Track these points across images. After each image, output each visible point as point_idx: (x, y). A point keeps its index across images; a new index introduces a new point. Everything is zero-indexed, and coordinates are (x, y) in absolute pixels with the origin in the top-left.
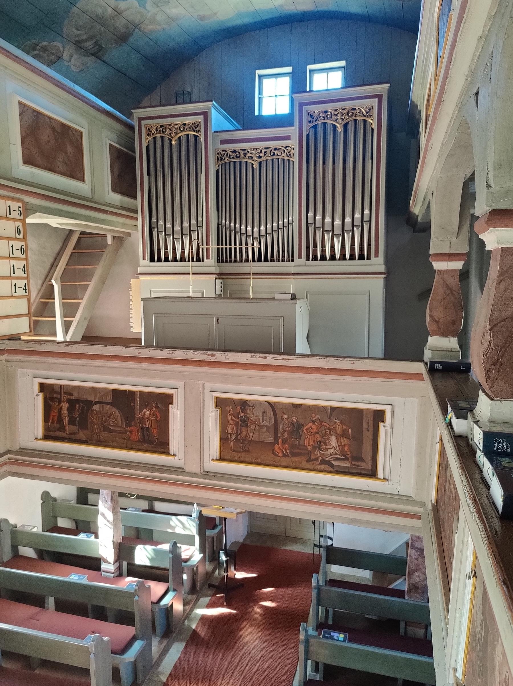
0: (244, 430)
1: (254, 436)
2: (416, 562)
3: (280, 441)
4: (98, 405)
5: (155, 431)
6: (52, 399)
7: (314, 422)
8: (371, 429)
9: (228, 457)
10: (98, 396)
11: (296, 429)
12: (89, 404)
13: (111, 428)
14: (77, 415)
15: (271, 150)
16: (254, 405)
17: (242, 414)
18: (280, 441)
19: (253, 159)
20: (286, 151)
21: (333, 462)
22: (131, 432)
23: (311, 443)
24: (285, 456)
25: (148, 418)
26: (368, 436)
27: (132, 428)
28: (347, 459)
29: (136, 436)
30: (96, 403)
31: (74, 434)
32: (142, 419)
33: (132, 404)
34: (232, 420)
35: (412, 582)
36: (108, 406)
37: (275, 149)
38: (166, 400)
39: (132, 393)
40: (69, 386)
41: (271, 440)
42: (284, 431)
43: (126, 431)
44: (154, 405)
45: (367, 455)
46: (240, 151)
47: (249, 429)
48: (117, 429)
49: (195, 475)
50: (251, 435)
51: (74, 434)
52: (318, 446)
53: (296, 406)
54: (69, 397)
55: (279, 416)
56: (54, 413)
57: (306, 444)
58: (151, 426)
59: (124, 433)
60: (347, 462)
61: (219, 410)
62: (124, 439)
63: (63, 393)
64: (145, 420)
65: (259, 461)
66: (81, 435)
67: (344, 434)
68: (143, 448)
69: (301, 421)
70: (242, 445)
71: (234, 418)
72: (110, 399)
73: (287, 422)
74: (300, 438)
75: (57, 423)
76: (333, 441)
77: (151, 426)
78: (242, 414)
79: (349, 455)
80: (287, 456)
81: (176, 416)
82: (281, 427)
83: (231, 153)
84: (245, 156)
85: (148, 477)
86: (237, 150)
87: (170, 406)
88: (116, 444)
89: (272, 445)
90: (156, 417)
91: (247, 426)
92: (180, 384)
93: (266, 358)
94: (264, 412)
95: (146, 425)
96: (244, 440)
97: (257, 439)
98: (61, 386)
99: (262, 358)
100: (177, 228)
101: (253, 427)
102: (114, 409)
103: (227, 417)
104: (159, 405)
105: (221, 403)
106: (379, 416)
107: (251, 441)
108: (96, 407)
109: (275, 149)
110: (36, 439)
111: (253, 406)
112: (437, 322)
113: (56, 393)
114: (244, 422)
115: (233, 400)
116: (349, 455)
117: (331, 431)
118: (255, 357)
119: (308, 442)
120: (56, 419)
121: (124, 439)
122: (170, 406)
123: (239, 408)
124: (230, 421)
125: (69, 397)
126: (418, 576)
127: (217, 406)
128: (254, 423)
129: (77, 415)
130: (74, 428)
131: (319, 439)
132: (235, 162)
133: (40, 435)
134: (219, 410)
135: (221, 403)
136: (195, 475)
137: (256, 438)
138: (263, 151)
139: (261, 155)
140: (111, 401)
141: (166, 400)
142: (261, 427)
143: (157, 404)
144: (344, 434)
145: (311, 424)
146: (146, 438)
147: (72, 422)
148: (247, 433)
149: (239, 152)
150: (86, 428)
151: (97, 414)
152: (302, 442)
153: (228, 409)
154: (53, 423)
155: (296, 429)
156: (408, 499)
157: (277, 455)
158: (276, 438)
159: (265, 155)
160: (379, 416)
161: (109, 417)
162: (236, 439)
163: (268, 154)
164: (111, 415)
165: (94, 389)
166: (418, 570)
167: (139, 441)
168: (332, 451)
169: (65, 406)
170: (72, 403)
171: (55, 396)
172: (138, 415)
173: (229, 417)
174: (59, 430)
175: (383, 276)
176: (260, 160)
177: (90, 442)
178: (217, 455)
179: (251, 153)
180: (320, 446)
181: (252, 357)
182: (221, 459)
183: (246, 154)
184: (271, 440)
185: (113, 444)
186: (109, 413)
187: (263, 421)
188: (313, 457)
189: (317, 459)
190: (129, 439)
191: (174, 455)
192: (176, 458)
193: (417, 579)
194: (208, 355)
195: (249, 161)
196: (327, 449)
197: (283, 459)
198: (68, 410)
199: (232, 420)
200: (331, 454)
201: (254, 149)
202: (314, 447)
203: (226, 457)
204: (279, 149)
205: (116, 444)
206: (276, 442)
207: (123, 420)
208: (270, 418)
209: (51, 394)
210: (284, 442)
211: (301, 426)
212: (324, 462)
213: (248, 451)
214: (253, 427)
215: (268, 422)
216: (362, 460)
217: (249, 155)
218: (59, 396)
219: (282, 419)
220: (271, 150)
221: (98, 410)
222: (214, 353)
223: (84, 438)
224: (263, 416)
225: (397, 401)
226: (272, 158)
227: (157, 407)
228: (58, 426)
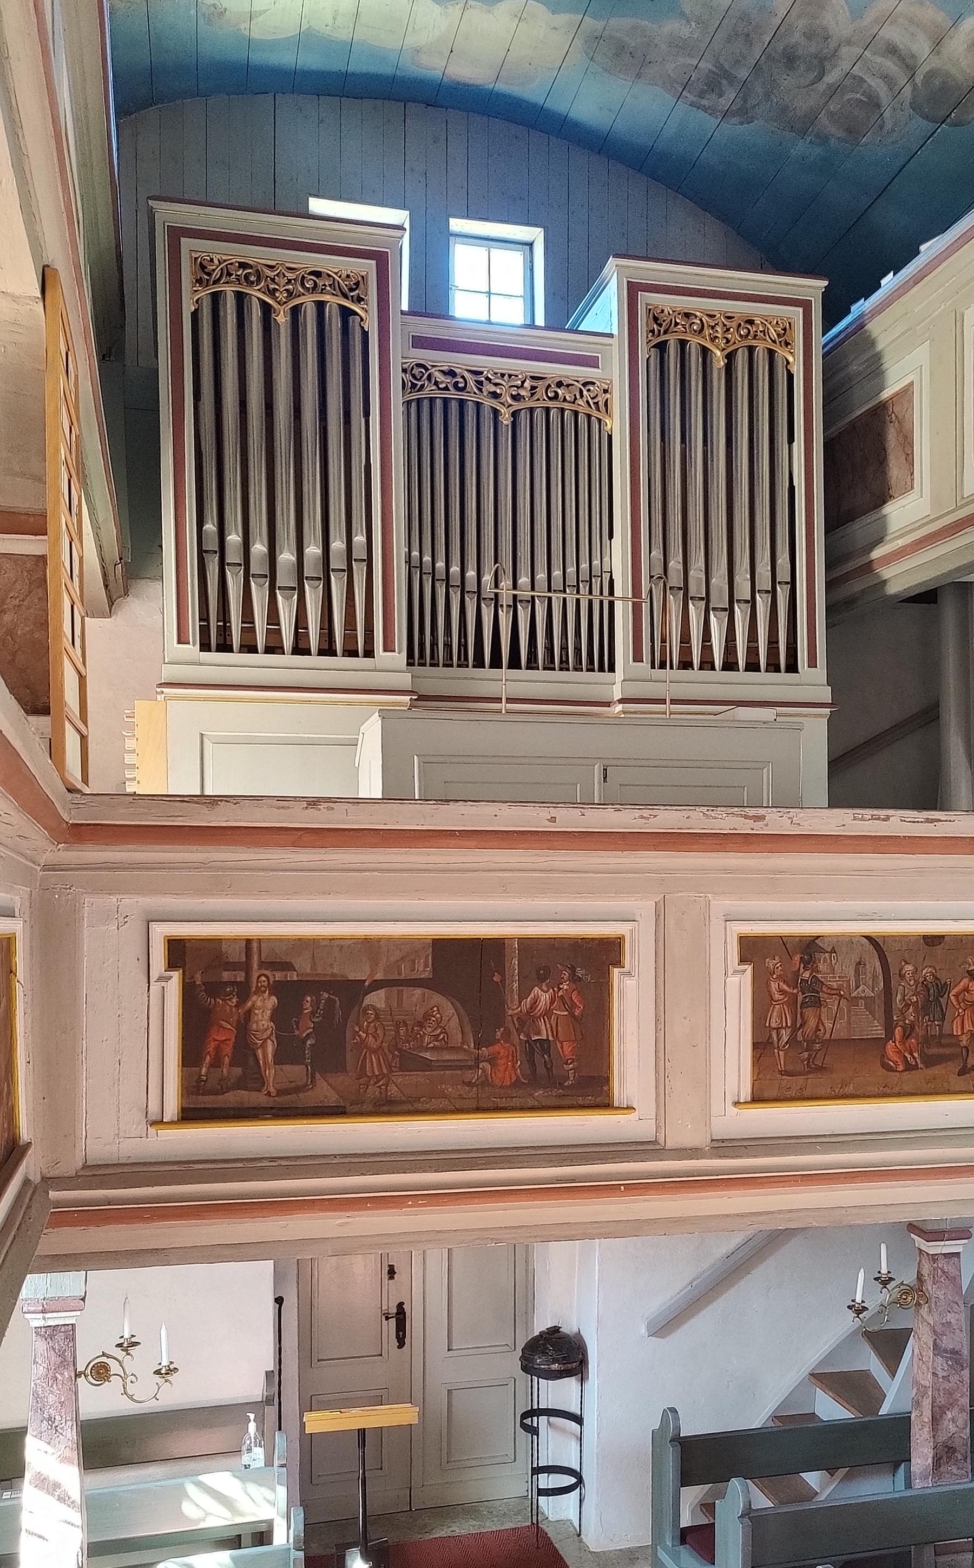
0: (810, 1013)
1: (837, 1026)
4: (382, 993)
5: (567, 1048)
6: (215, 989)
9: (774, 1093)
10: (382, 964)
11: (934, 995)
12: (353, 992)
13: (428, 1055)
14: (306, 1028)
15: (549, 386)
17: (807, 975)
19: (502, 400)
20: (585, 392)
22: (492, 1061)
25: (548, 1013)
27: (497, 1047)
29: (508, 1070)
30: (377, 985)
31: (298, 1090)
32: (528, 1020)
33: (497, 978)
34: (782, 991)
36: (418, 991)
37: (560, 384)
38: (604, 954)
39: (496, 945)
40: (279, 940)
41: (878, 1031)
42: (907, 1006)
43: (478, 1060)
44: (566, 975)
46: (466, 374)
47: (824, 1010)
48: (447, 1056)
49: (693, 1153)
50: (829, 1025)
51: (298, 1090)
53: (932, 941)
54: (279, 976)
55: (894, 970)
56: (223, 1034)
58: (556, 1036)
59: (470, 1068)
61: (749, 969)
62: (469, 1084)
63: (255, 966)
64: (535, 1019)
66: (324, 1091)
68: (531, 1102)
69: (944, 977)
70: (806, 1055)
71: (785, 987)
72: (424, 970)
73: (912, 983)
74: (943, 1019)
75: (231, 1065)
77: (556, 1036)
78: (807, 975)
81: (631, 997)
82: (899, 997)
83: (440, 377)
84: (480, 390)
85: (559, 1180)
86: (457, 371)
87: (616, 971)
88: (444, 1103)
90: (571, 1008)
92: (644, 907)
93: (887, 819)
94: (859, 963)
95: (539, 1033)
96: (811, 1042)
97: (844, 1035)
98: (249, 941)
99: (879, 819)
100: (286, 557)
101: (833, 1003)
102: (437, 999)
103: (768, 986)
104: (580, 972)
105: (751, 949)
107: (830, 1040)
108: (377, 999)
109: (560, 384)
110: (159, 1123)
113: (232, 966)
114: (809, 994)
115: (782, 941)
118: (863, 819)
120: (228, 1050)
121: (469, 1084)
122: (616, 971)
123: (797, 958)
124: (777, 996)
125: (279, 976)
127: (742, 960)
128: (837, 993)
129: (306, 1028)
130: (295, 1072)
132: (446, 401)
133: (172, 1109)
134: (749, 969)
135: (751, 949)
136: (693, 1153)
137: (841, 1030)
138: (527, 384)
139: (523, 393)
140: (427, 974)
141: (604, 954)
142: (853, 1001)
143: (573, 969)
146: (541, 1070)
147: (287, 1053)
149: (463, 377)
150: (341, 1067)
151: (377, 1017)
152: (946, 1030)
153: (770, 963)
154: (216, 1063)
159: (532, 395)
161: (421, 1025)
162: (792, 1040)
163: (540, 392)
164: (427, 1016)
165: (370, 945)
167: (516, 1084)
169: (264, 1006)
170: (290, 994)
171: (226, 976)
172: (515, 1007)
173: (774, 986)
174: (240, 1084)
176: (517, 406)
177: (356, 1108)
178: (746, 1094)
179: (496, 385)
181: (855, 819)
182: (757, 1099)
183: (481, 383)
185: (434, 1103)
186: (420, 1012)
187: (857, 987)
190: (485, 1083)
191: (630, 1108)
192: (633, 1116)
194: (746, 817)
195: (488, 402)
198: (276, 1016)
199: (782, 991)
201: (503, 375)
203: (766, 1095)
204: (568, 386)
205: (444, 1103)
207: (468, 1028)
208: (874, 977)
209: (209, 977)
213: (821, 1069)
214: (833, 1003)
215: (870, 989)
217: (493, 389)
218: (241, 976)
220: (549, 386)
221: (381, 1005)
222: (761, 812)
223: (332, 1098)
226: (550, 404)
227: (574, 979)
228: (238, 1071)
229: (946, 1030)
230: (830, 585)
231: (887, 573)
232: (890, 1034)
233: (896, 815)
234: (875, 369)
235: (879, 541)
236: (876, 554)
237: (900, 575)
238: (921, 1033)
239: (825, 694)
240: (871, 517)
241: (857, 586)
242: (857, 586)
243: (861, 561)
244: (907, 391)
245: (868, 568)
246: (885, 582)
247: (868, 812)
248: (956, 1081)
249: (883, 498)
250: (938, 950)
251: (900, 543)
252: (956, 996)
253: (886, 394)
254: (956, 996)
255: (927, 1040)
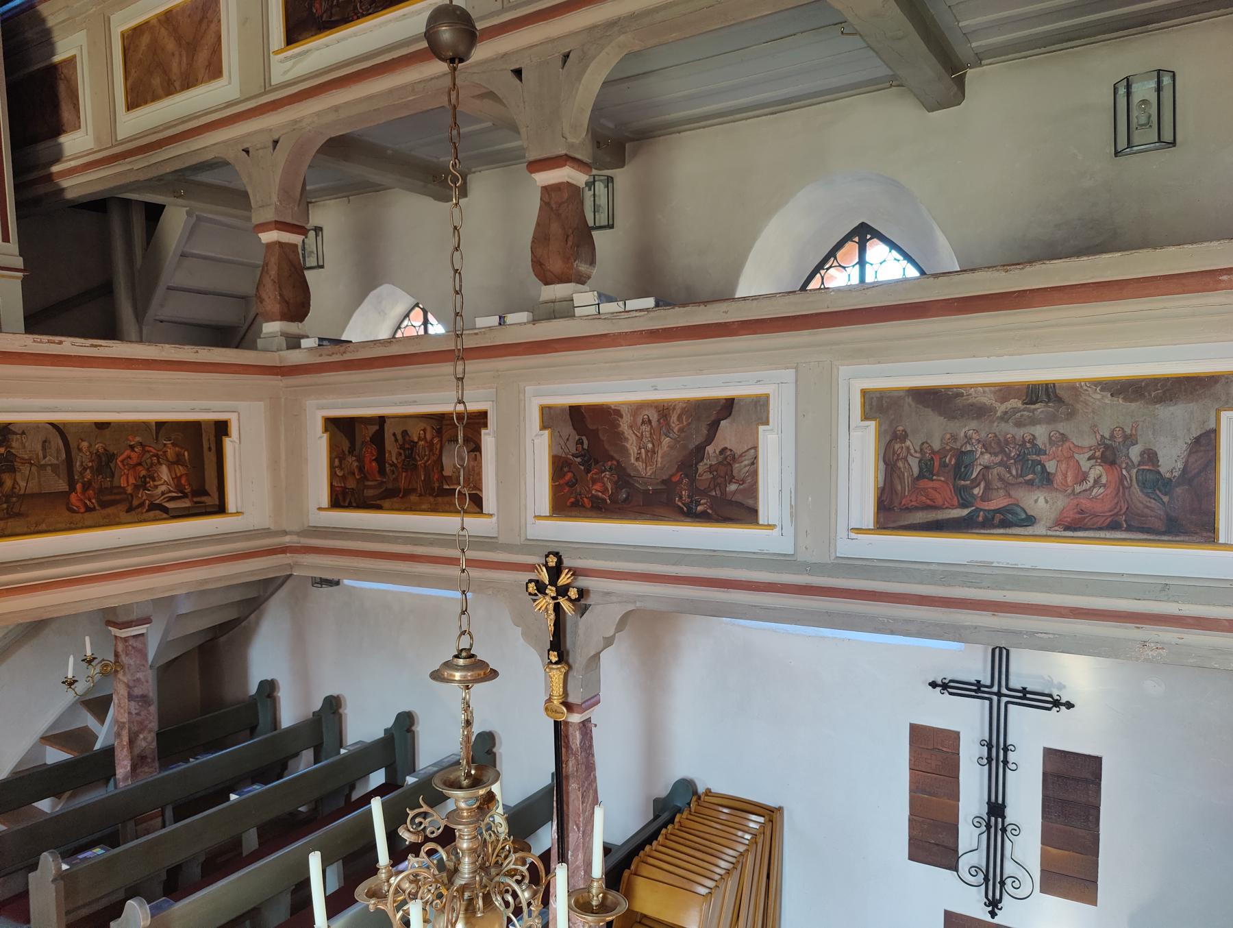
1: (30, 485)
2: (139, 718)
3: (79, 486)
7: (132, 447)
8: (213, 448)
16: (25, 430)
18: (79, 486)
21: (167, 505)
23: (132, 481)
24: (89, 510)
26: (209, 458)
28: (185, 496)
35: (137, 751)
41: (63, 486)
42: (85, 469)
45: (211, 485)
47: (18, 474)
50: (23, 484)
52: (142, 484)
55: (73, 444)
57: (123, 484)
60: (186, 500)
65: (44, 527)
67: (178, 461)
69: (112, 449)
70: (5, 506)
74: (113, 476)
76: (164, 473)
79: (188, 489)
80: (94, 509)
89: (65, 495)
91: (13, 470)
94: (45, 442)
97: (36, 490)
101: (25, 469)
106: (222, 428)
111: (23, 433)
112: (287, 303)
116: (188, 489)
117: (159, 458)
119: (126, 481)
126: (145, 739)
131: (143, 473)
137: (33, 487)
142: (43, 467)
144: (178, 461)
145: (128, 452)
148: (15, 482)
155: (104, 462)
156: (267, 533)
157: (74, 511)
158: (72, 484)
160: (222, 428)
166: (141, 731)
168: (163, 488)
175: (21, 274)
180: (146, 483)
184: (63, 486)
187: (45, 457)
188: (135, 503)
189: (142, 505)
193: (144, 744)
196: (156, 487)
197: (87, 515)
200: (163, 493)
202: (136, 487)
206: (72, 488)
208: (58, 451)
210: (87, 486)
211: (111, 457)
212: (154, 507)
213: (19, 515)
214: (25, 469)
216: (206, 493)
219: (80, 450)
224: (44, 449)
225: (242, 405)
229: (116, 483)
230: (17, 188)
231: (65, 183)
232: (72, 488)
233: (68, 341)
234: (46, 40)
235: (58, 159)
236: (55, 169)
237: (75, 186)
238: (96, 486)
239: (19, 262)
240: (49, 143)
241: (41, 190)
242: (41, 190)
243: (42, 173)
244: (71, 61)
245: (49, 178)
246: (63, 190)
247: (45, 338)
248: (124, 516)
249: (58, 130)
250: (107, 432)
251: (73, 164)
252: (122, 462)
253: (57, 59)
254: (122, 462)
255: (101, 491)
